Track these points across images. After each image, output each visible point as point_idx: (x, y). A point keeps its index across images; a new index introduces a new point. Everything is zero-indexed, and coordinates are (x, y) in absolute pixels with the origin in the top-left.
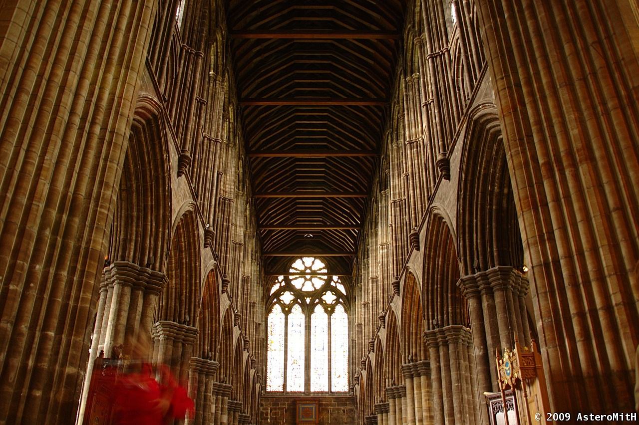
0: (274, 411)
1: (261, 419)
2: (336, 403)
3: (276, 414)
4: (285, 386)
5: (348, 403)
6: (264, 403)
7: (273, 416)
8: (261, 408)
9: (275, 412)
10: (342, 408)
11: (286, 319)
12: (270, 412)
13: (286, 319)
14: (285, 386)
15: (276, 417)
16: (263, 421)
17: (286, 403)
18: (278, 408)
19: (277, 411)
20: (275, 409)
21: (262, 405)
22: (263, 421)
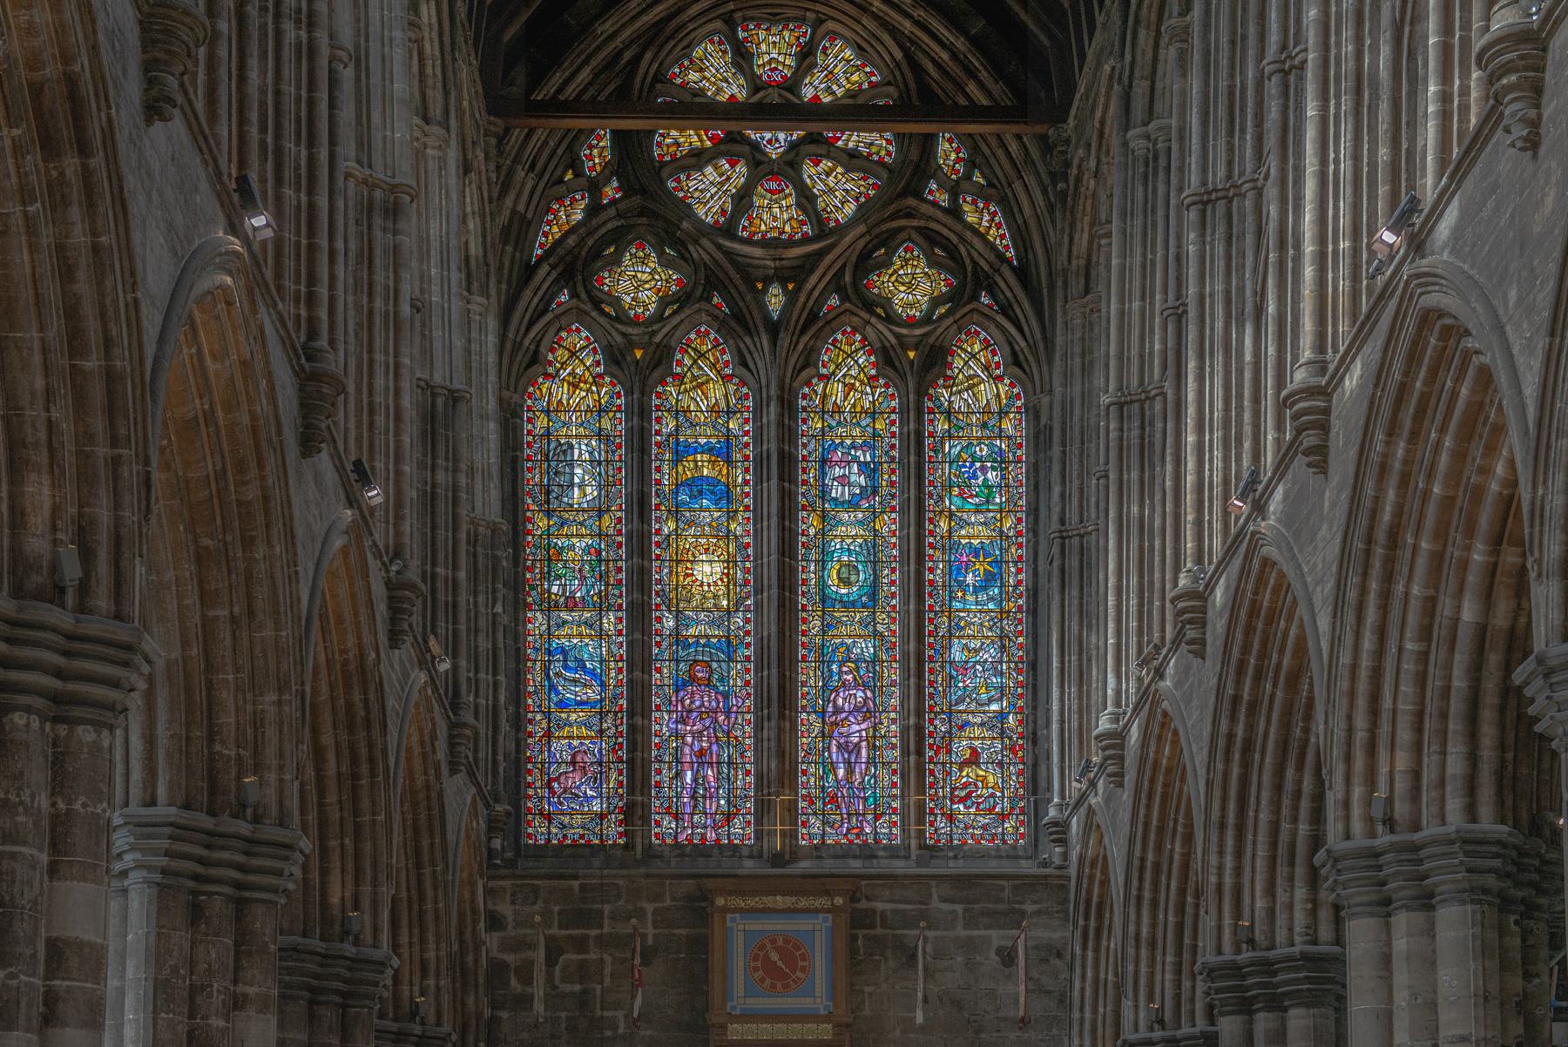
0: (574, 957)
1: (495, 1005)
2: (959, 908)
3: (583, 972)
4: (635, 813)
5: (1030, 908)
6: (506, 909)
7: (567, 988)
8: (492, 941)
9: (583, 965)
10: (997, 937)
11: (640, 416)
12: (551, 961)
13: (640, 416)
14: (635, 813)
15: (584, 992)
16: (504, 1015)
17: (649, 908)
18: (599, 938)
19: (593, 956)
20: (581, 944)
21: (495, 922)
22: (504, 1015)
